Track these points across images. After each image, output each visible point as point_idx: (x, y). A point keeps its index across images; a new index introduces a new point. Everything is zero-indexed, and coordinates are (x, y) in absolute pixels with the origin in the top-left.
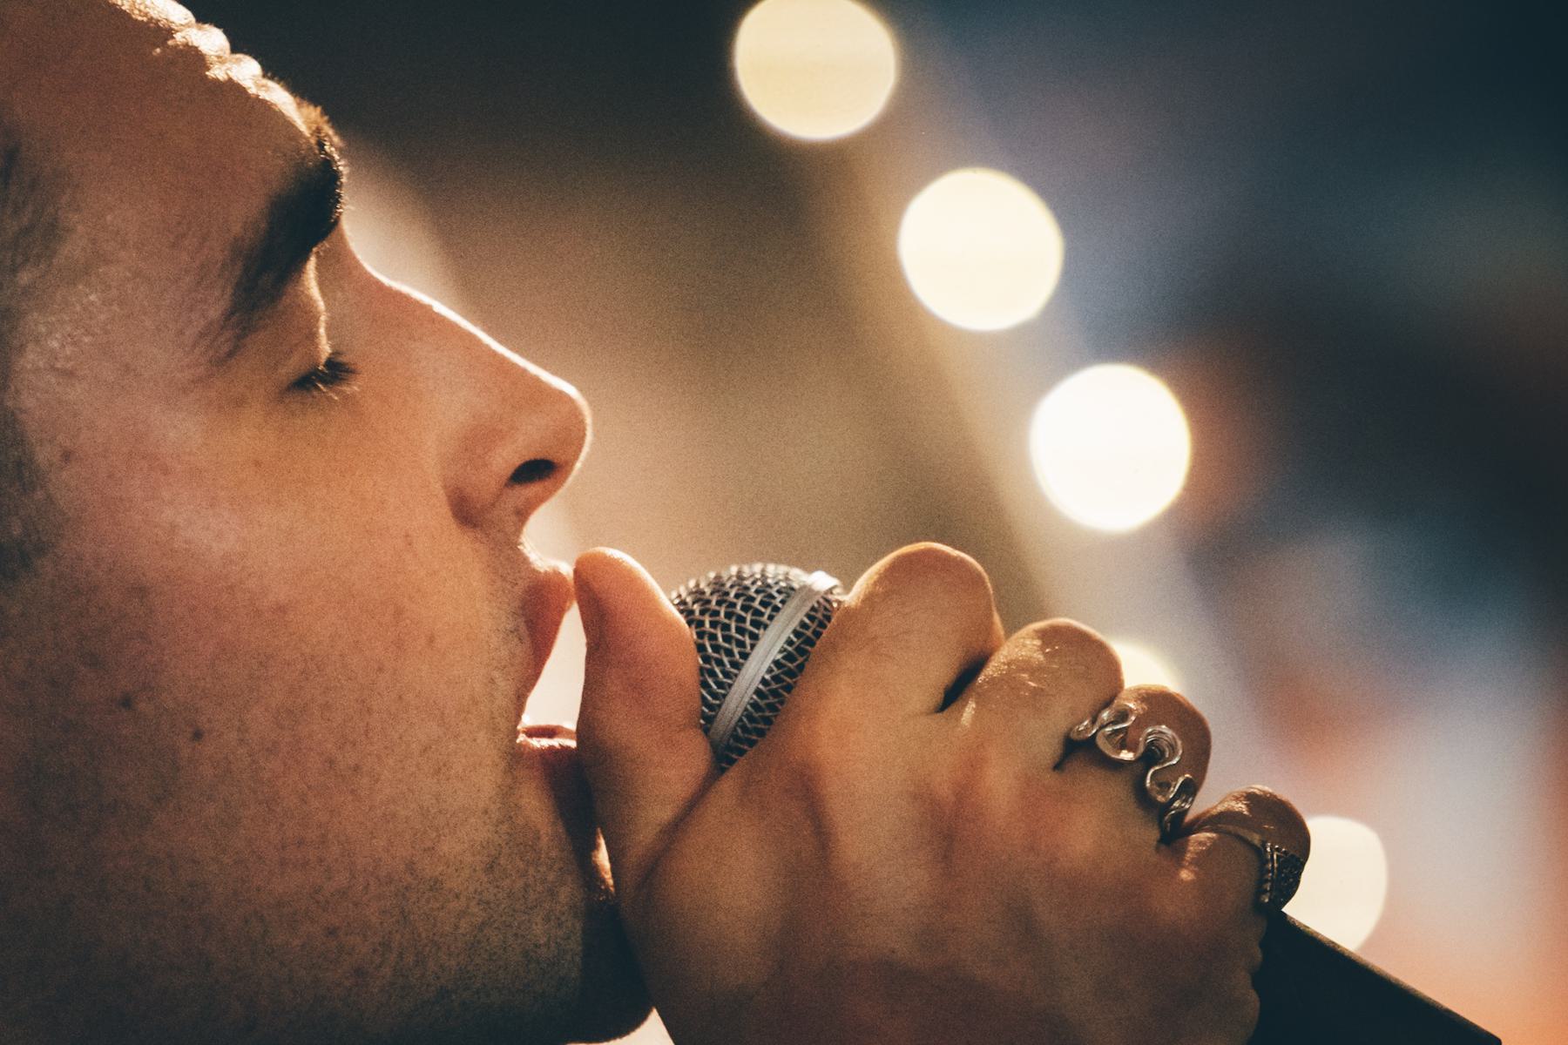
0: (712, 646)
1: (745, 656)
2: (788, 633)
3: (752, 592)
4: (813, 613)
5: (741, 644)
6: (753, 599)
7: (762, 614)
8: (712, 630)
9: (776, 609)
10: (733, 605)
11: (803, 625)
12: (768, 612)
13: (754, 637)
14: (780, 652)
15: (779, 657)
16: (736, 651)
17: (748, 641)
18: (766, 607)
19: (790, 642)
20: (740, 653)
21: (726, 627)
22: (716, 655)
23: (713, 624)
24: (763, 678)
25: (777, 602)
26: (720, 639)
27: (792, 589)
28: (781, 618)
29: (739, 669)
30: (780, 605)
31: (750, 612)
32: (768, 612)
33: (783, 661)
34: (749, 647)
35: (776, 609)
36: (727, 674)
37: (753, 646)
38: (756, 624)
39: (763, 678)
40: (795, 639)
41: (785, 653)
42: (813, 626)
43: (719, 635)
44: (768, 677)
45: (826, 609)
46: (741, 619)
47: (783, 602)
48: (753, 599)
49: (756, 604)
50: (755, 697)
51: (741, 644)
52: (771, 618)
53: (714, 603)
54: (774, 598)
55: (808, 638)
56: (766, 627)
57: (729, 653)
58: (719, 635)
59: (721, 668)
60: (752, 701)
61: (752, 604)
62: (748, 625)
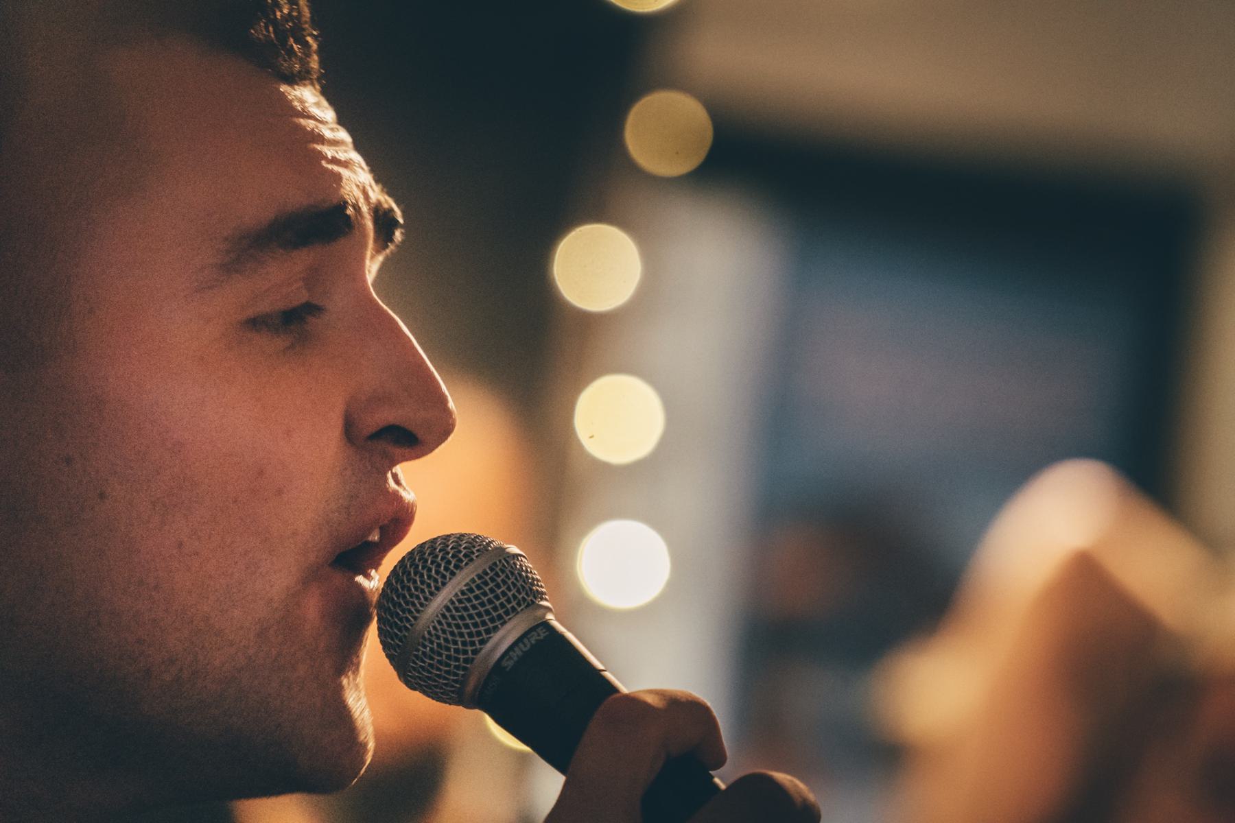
0: (427, 575)
1: (444, 584)
2: (473, 576)
6: (448, 553)
7: (462, 561)
8: (431, 566)
9: (472, 560)
12: (465, 561)
13: (453, 574)
14: (465, 586)
15: (464, 588)
16: (440, 580)
17: (448, 575)
19: (473, 581)
21: (449, 562)
22: (435, 576)
24: (451, 600)
25: (474, 557)
26: (442, 568)
27: (487, 550)
28: (471, 566)
30: (475, 558)
32: (465, 561)
33: (467, 592)
34: (448, 579)
35: (472, 560)
37: (450, 579)
39: (451, 600)
40: (477, 579)
43: (443, 565)
44: (453, 598)
45: (504, 565)
47: (477, 556)
48: (460, 552)
50: (444, 610)
51: (444, 577)
52: (466, 564)
54: (473, 553)
56: (462, 568)
57: (436, 581)
58: (443, 565)
59: (435, 584)
60: (442, 612)
61: (447, 556)
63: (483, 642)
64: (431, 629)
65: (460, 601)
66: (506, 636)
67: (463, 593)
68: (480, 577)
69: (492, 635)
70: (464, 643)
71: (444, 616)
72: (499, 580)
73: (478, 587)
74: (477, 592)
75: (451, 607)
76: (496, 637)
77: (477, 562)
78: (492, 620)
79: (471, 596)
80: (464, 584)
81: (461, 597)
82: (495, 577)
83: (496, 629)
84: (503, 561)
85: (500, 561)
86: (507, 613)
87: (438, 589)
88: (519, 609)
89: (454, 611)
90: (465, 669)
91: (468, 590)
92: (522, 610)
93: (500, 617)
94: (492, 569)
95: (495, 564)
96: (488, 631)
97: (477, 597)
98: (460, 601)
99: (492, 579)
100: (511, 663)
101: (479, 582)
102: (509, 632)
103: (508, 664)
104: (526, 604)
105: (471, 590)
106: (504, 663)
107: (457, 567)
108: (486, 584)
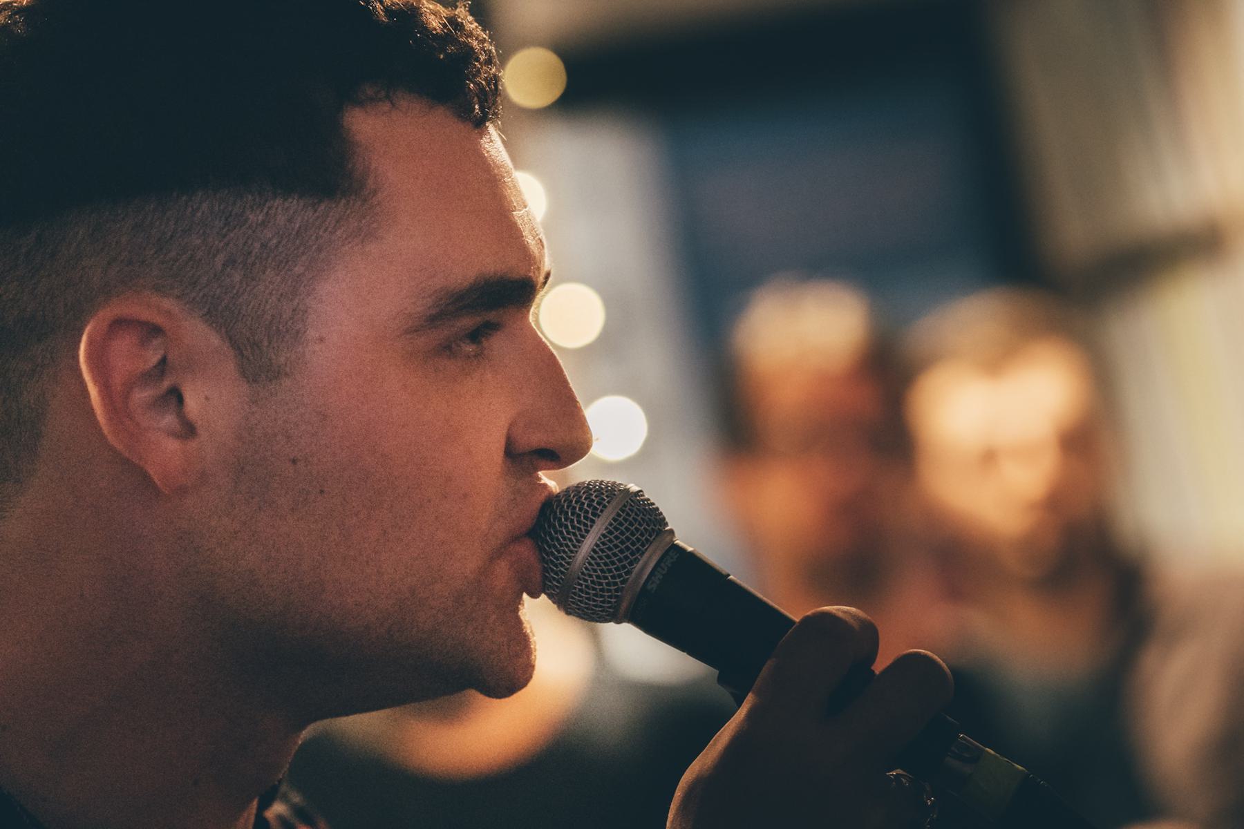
0: (571, 526)
1: (587, 531)
3: (593, 497)
4: (624, 508)
5: (585, 525)
9: (605, 506)
10: (583, 504)
11: (619, 515)
13: (593, 521)
15: (604, 532)
18: (599, 505)
19: (611, 524)
20: (585, 530)
22: (578, 525)
23: (580, 509)
25: (605, 502)
27: (615, 495)
29: (584, 538)
30: (607, 504)
31: (576, 516)
32: (600, 508)
35: (605, 506)
36: (575, 546)
37: (591, 526)
38: (594, 514)
41: (607, 531)
42: (624, 515)
44: (598, 543)
45: (631, 505)
46: (587, 512)
47: (608, 502)
48: (593, 501)
49: (595, 504)
50: (592, 553)
52: (602, 511)
53: (583, 498)
55: (611, 530)
56: (599, 516)
59: (582, 533)
62: (590, 516)
63: (629, 573)
64: (584, 569)
65: (604, 544)
66: (649, 560)
67: (604, 536)
68: (615, 520)
69: (635, 565)
70: (613, 577)
71: (592, 558)
72: (631, 519)
73: (616, 529)
74: (616, 533)
75: (597, 549)
76: (638, 567)
77: (610, 508)
78: (633, 554)
79: (612, 537)
80: (604, 528)
81: (603, 540)
82: (627, 517)
83: (637, 560)
84: (629, 501)
85: (627, 502)
86: (643, 545)
87: (583, 537)
88: (651, 539)
89: (600, 553)
90: (617, 597)
91: (608, 533)
92: (654, 539)
93: (638, 550)
94: (623, 511)
95: (625, 506)
96: (631, 564)
97: (617, 538)
98: (604, 544)
99: (625, 520)
100: (654, 586)
101: (615, 524)
102: (650, 557)
103: (652, 587)
104: (655, 533)
105: (610, 532)
106: (649, 587)
107: (594, 514)
108: (621, 524)
